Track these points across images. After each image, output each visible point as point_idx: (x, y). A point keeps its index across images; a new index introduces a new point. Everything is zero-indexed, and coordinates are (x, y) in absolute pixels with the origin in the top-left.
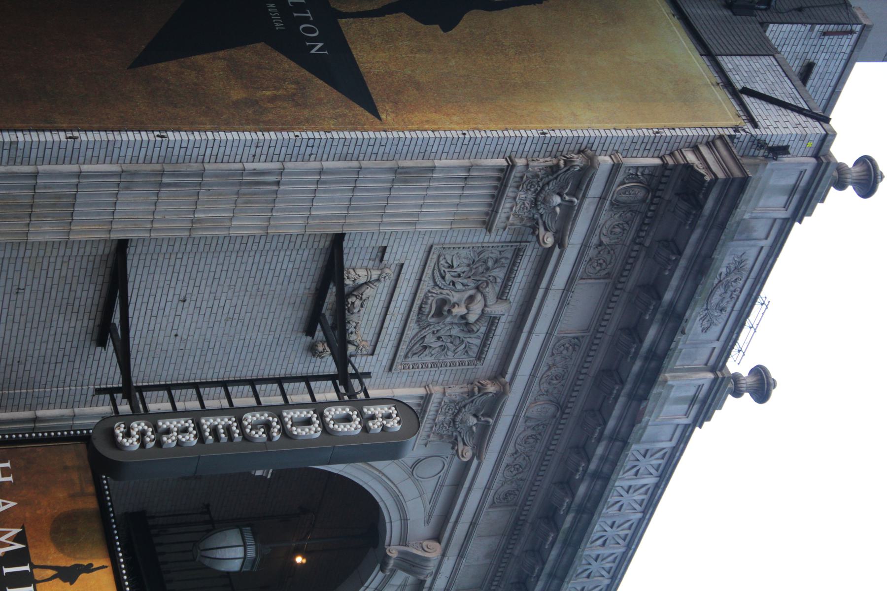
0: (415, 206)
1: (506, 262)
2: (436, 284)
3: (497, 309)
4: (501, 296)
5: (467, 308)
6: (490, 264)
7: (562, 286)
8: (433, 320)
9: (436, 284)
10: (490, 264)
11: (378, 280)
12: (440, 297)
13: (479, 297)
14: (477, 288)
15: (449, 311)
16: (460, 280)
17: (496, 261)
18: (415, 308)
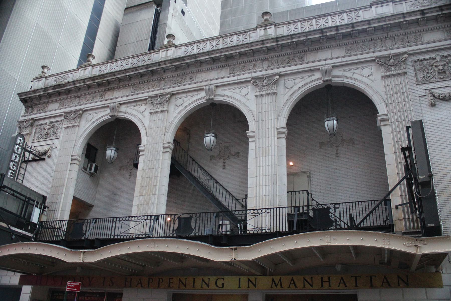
0: (400, 94)
1: (421, 63)
2: (433, 77)
3: (438, 58)
4: (434, 58)
5: (439, 66)
6: (422, 66)
7: (425, 45)
8: (447, 73)
9: (433, 77)
10: (422, 66)
11: (432, 93)
12: (437, 74)
13: (435, 64)
14: (432, 66)
15: (442, 70)
16: (429, 72)
17: (421, 65)
18: (443, 80)
